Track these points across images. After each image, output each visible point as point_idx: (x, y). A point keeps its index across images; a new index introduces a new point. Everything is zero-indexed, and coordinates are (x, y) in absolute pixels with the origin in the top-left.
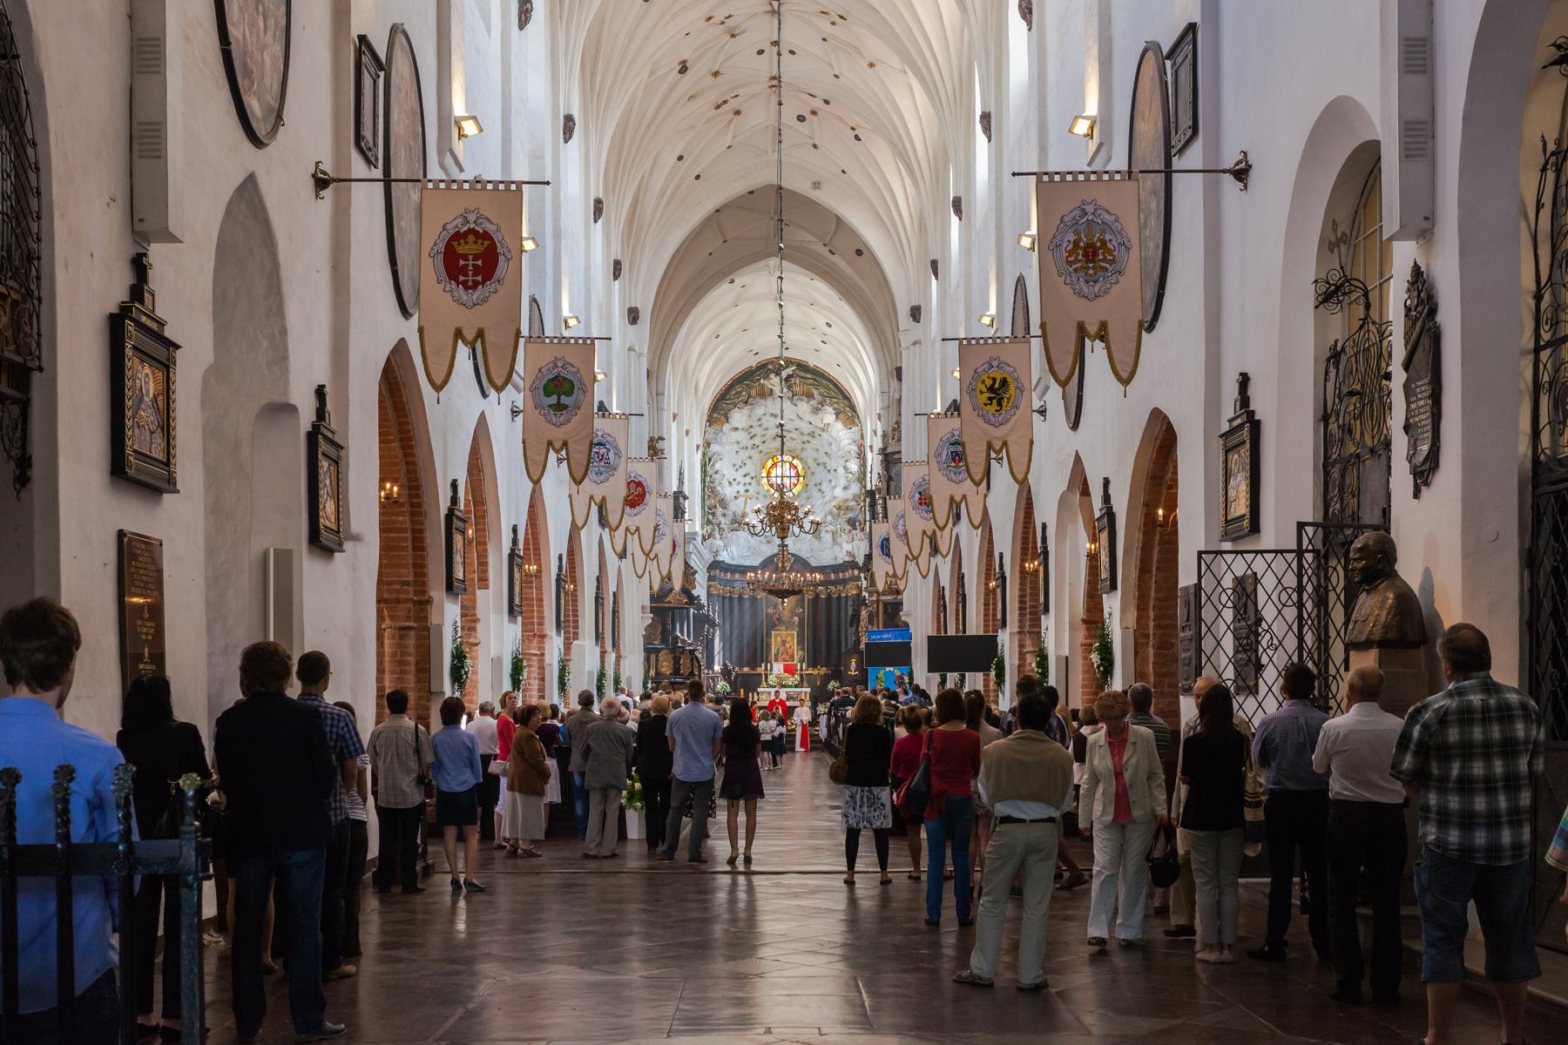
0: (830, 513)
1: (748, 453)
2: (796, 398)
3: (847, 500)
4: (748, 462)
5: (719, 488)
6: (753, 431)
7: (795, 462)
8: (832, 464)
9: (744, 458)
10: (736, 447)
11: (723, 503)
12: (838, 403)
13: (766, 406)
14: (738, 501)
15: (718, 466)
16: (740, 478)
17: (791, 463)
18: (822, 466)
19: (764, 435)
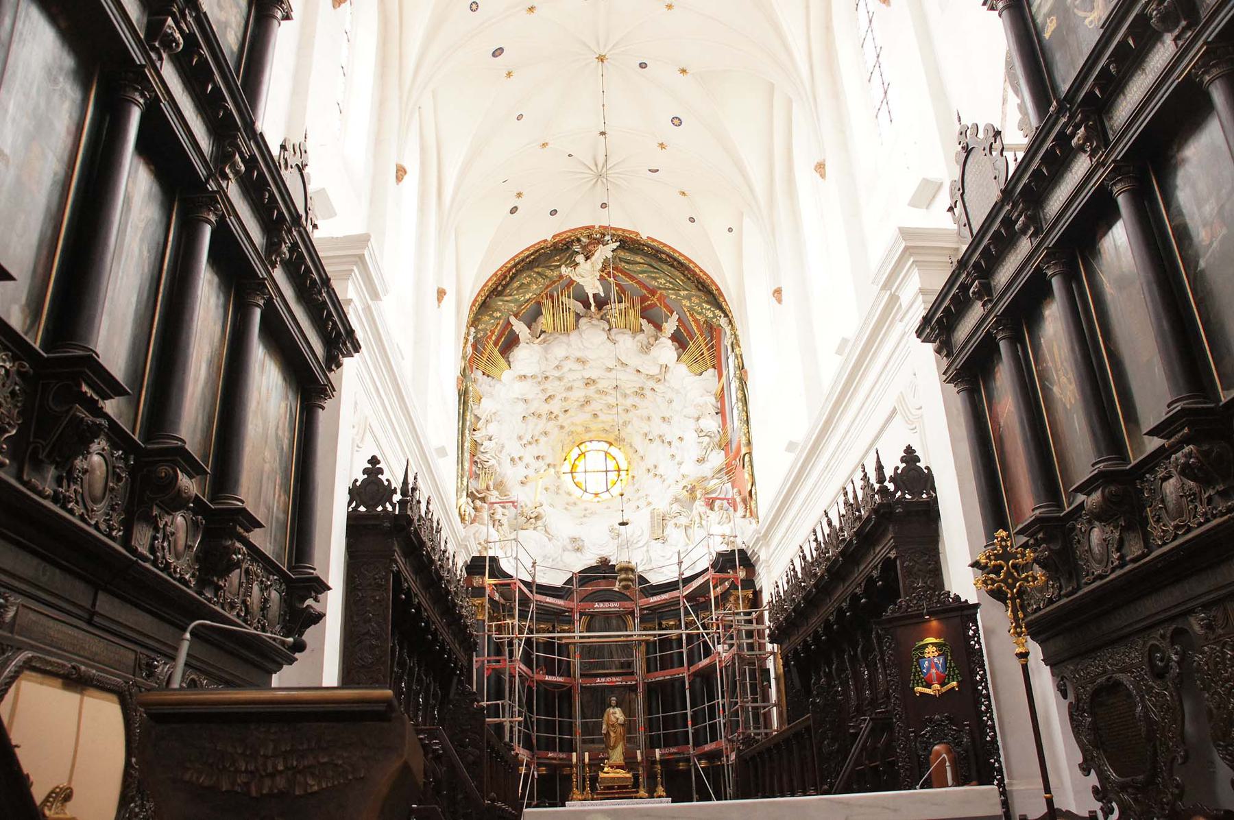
0: (676, 500)
1: (542, 425)
2: (614, 331)
3: (704, 479)
4: (543, 440)
5: (492, 462)
6: (552, 387)
7: (613, 450)
8: (671, 433)
9: (537, 433)
10: (520, 408)
11: (500, 486)
12: (689, 298)
13: (569, 345)
14: (527, 488)
15: (492, 429)
16: (529, 458)
17: (606, 453)
18: (657, 442)
19: (566, 399)
